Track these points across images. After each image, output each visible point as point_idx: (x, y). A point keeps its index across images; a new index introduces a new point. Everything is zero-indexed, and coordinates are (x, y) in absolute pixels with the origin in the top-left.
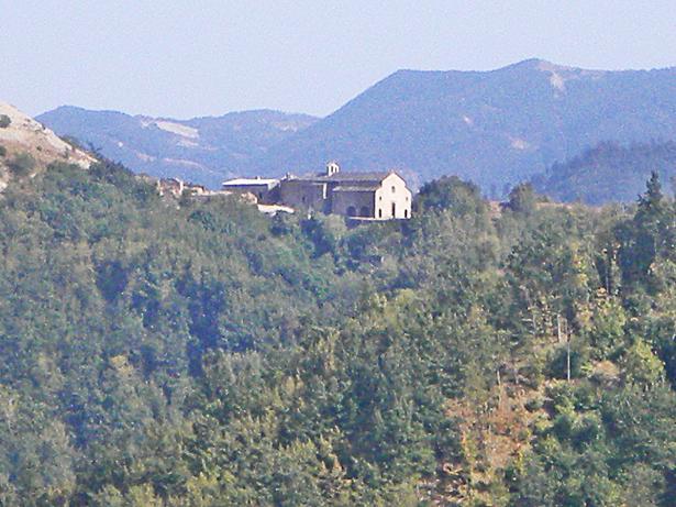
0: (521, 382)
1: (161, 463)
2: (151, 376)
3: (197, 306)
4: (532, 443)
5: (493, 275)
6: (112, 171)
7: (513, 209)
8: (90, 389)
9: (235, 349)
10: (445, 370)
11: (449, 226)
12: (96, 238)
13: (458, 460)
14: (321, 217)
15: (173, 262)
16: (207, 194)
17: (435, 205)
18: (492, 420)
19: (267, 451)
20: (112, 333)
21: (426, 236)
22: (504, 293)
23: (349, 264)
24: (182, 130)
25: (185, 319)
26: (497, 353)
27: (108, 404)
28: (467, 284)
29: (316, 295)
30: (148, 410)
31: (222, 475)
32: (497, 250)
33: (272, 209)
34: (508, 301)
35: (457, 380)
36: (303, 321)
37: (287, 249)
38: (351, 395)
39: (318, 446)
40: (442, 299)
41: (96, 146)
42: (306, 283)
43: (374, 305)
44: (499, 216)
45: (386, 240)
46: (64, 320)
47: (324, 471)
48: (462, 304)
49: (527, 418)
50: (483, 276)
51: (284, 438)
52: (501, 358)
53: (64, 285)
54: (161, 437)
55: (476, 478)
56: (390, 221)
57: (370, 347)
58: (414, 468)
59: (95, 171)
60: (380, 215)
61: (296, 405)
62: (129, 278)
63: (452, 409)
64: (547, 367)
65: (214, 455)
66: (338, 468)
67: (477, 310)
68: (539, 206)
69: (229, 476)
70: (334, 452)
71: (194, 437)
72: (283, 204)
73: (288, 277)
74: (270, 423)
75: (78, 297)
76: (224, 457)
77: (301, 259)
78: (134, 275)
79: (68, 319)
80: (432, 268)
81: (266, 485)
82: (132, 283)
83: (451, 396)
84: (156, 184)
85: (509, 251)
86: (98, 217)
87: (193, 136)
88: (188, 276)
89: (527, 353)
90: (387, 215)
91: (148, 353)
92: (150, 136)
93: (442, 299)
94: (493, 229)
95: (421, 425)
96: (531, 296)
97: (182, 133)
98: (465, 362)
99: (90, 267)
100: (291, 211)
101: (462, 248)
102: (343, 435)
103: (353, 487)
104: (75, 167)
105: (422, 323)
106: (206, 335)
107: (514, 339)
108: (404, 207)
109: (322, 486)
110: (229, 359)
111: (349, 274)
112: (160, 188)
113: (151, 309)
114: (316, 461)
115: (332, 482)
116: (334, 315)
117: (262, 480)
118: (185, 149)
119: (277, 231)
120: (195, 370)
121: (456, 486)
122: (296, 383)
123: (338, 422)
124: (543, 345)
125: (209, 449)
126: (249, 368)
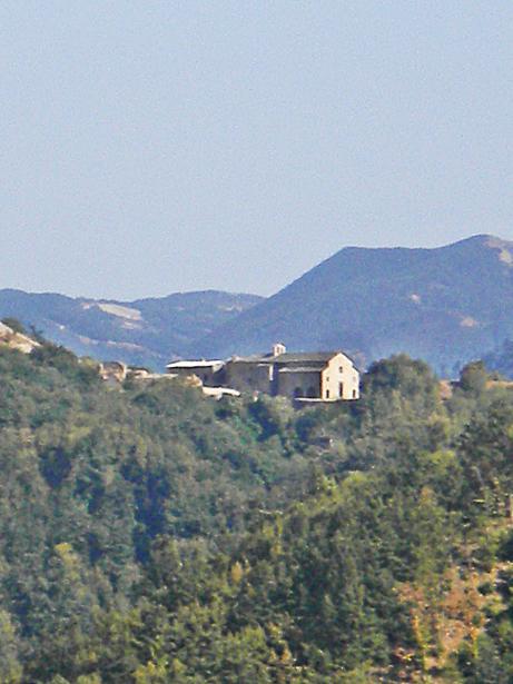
0: (474, 565)
1: (108, 650)
2: (96, 564)
3: (141, 492)
4: (487, 626)
5: (445, 456)
6: (54, 355)
7: (465, 389)
8: (36, 577)
9: (182, 535)
10: (396, 554)
11: (400, 409)
12: (37, 424)
13: (412, 644)
14: (267, 398)
15: (117, 447)
16: (151, 376)
17: (383, 385)
18: (446, 603)
19: (217, 639)
20: (57, 519)
21: (374, 417)
22: (455, 474)
23: (297, 447)
24: (125, 312)
25: (130, 505)
26: (449, 535)
27: (52, 592)
28: (417, 466)
29: (264, 479)
30: (94, 597)
31: (171, 662)
32: (447, 430)
33: (218, 392)
34: (459, 483)
35: (408, 564)
36: (252, 504)
37: (235, 433)
38: (301, 581)
39: (268, 632)
40: (392, 480)
41: (38, 329)
42: (253, 466)
43: (322, 489)
44: (449, 395)
45: (334, 422)
46: (7, 507)
47: (274, 657)
48: (412, 486)
49: (482, 601)
50: (435, 457)
51: (233, 625)
52: (453, 541)
53: (9, 472)
54: (108, 625)
55: (429, 662)
56: (337, 401)
57: (320, 531)
58: (365, 653)
59: (36, 355)
60: (328, 396)
61: (244, 591)
62: (72, 464)
63: (404, 592)
64: (501, 549)
65: (163, 643)
66: (288, 655)
67: (427, 491)
68: (490, 385)
69: (178, 664)
70: (285, 638)
71: (141, 625)
72: (228, 387)
73: (234, 459)
74: (218, 609)
75: (21, 484)
76: (173, 645)
77: (249, 442)
78: (77, 461)
79: (13, 505)
80: (381, 450)
81: (216, 673)
82: (76, 468)
83: (402, 579)
84: (99, 368)
85: (461, 431)
86: (39, 401)
87: (135, 318)
88: (134, 461)
89: (480, 534)
90: (334, 396)
91: (93, 538)
92: (91, 320)
93: (392, 480)
94: (444, 409)
95: (373, 610)
96: (483, 476)
97: (123, 315)
98: (418, 544)
99: (33, 452)
100: (237, 393)
101: (411, 428)
102: (293, 621)
103: (304, 674)
104: (16, 351)
105: (373, 506)
106: (152, 519)
107: (465, 521)
108: (351, 390)
109: (273, 674)
110: (176, 545)
111: (298, 457)
112: (103, 372)
113: (97, 497)
114: (266, 648)
115: (282, 668)
116: (281, 498)
117: (212, 668)
118: (128, 331)
119: (223, 414)
120: (141, 556)
121: (409, 672)
122: (244, 567)
123: (287, 608)
124: (496, 526)
125: (158, 637)
126: (195, 553)
